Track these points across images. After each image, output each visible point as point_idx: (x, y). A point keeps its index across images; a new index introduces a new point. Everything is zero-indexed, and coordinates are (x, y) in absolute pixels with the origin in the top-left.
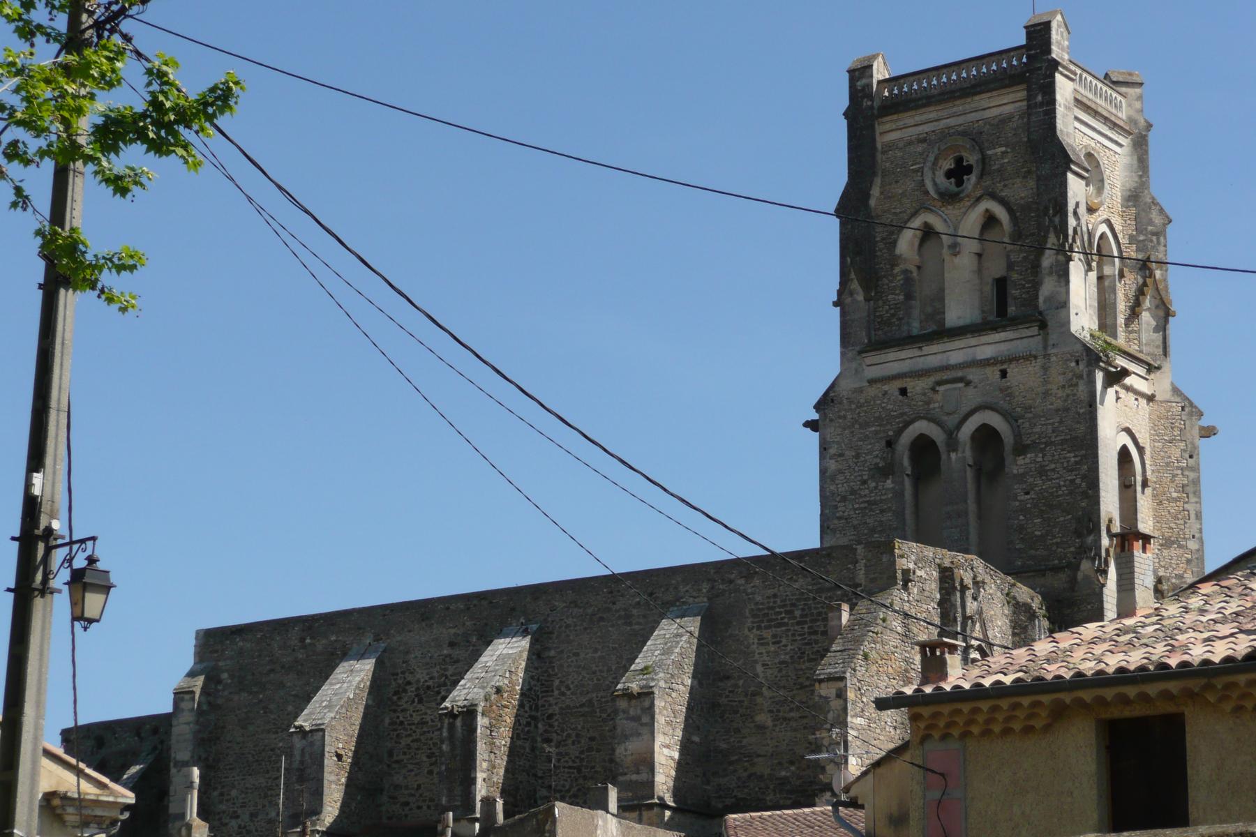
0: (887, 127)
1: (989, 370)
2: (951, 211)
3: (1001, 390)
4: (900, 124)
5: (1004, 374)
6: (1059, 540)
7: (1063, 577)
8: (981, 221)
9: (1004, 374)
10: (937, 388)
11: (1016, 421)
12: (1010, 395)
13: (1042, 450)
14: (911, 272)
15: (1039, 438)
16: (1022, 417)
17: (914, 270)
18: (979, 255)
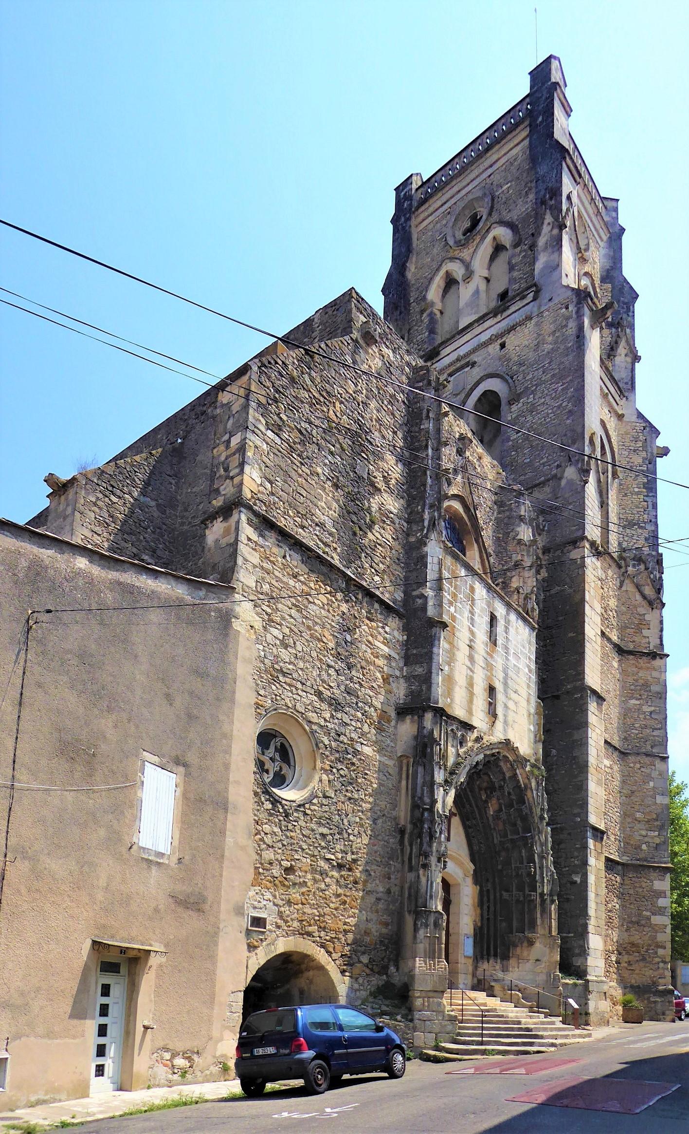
0: (422, 216)
1: (491, 349)
2: (465, 254)
3: (500, 359)
4: (431, 209)
5: (503, 346)
6: (545, 460)
7: (547, 489)
8: (490, 250)
9: (503, 346)
10: (449, 379)
11: (512, 378)
12: (509, 360)
13: (533, 392)
14: (435, 314)
15: (531, 384)
16: (517, 372)
17: (438, 313)
18: (488, 280)
